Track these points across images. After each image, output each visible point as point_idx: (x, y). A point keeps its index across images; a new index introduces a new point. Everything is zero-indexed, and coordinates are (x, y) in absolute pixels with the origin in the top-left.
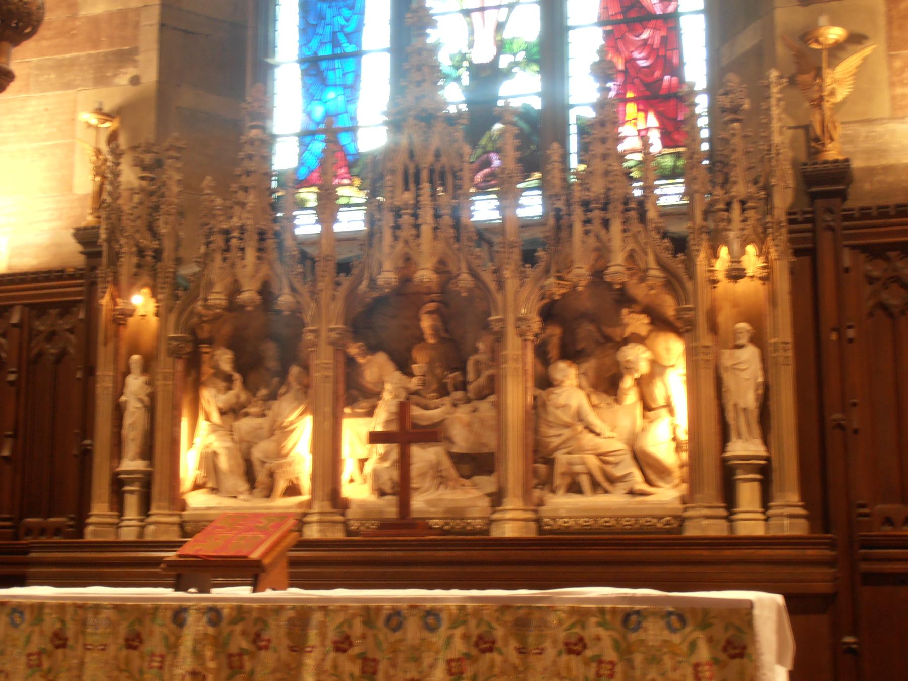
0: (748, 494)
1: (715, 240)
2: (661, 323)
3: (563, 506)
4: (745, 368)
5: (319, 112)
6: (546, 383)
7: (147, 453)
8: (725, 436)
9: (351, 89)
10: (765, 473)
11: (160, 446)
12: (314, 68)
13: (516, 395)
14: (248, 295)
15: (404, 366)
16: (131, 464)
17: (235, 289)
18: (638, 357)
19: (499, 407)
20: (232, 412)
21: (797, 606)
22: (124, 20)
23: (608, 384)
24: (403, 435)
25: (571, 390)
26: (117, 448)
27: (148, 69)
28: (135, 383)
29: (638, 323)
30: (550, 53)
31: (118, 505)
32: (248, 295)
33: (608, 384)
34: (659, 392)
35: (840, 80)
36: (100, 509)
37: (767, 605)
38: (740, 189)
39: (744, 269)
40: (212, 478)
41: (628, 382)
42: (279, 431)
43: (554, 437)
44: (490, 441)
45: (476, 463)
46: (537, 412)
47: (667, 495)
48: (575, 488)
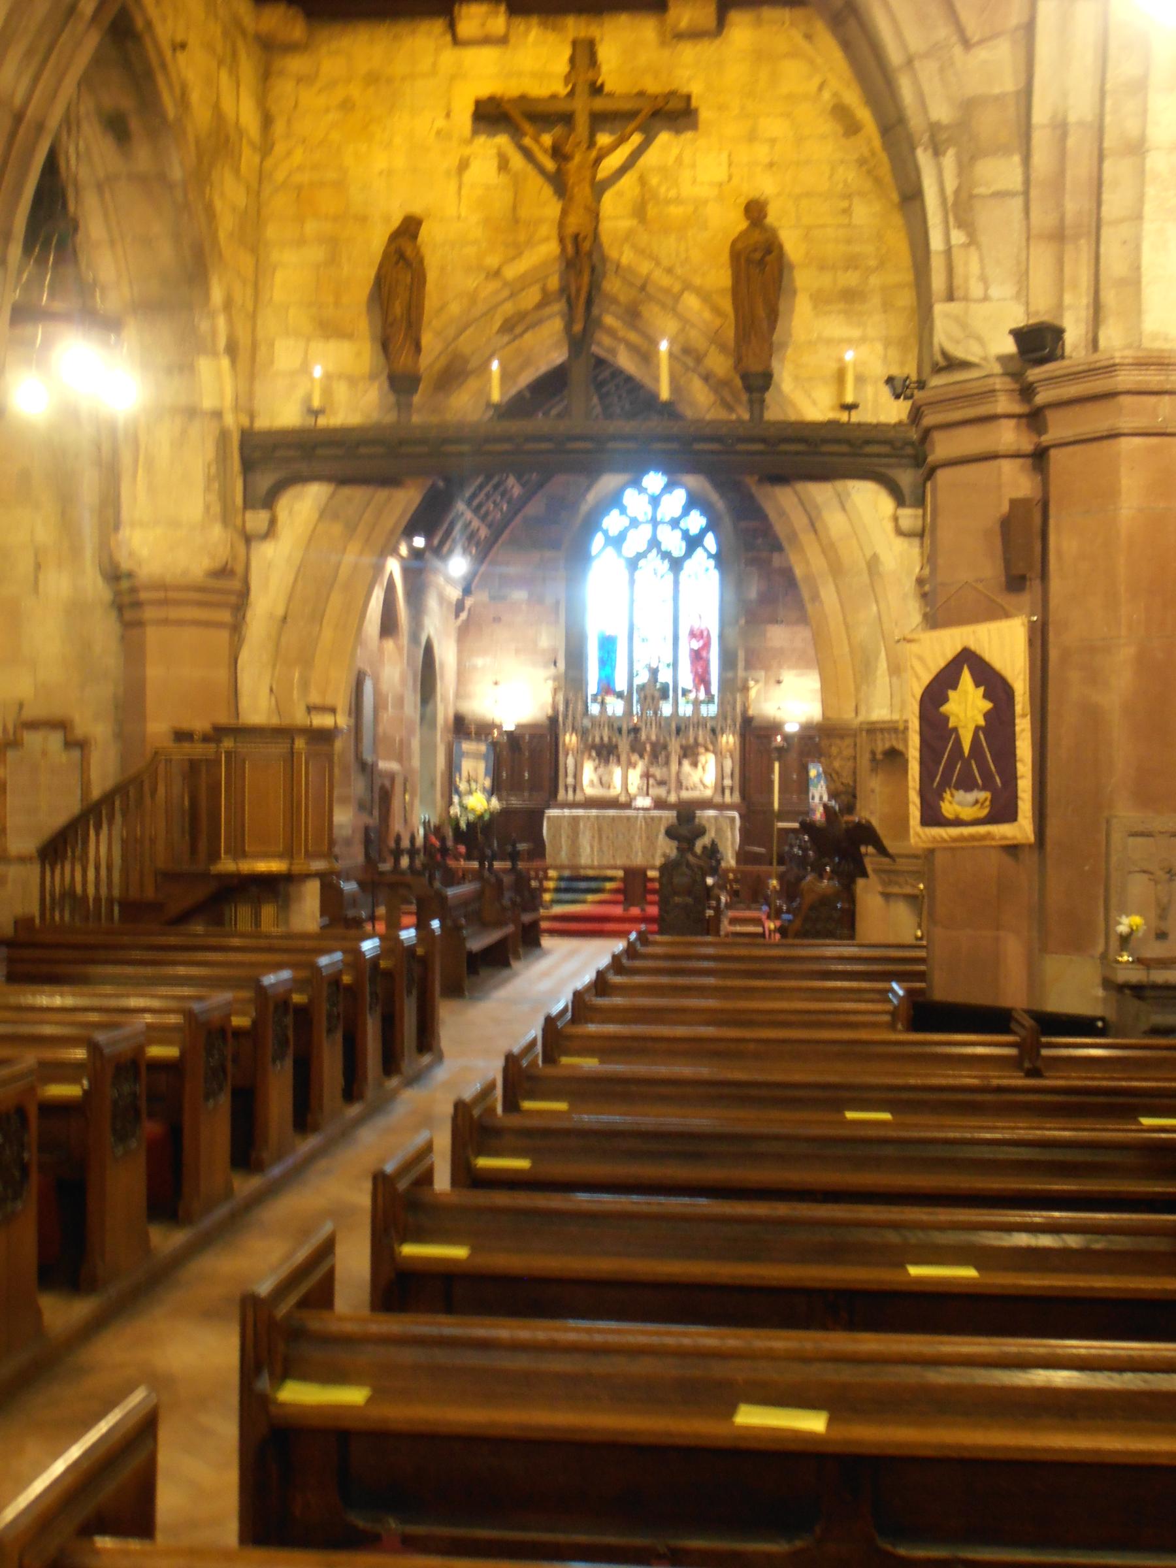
0: (727, 792)
1: (723, 732)
2: (707, 750)
3: (685, 795)
4: (728, 764)
5: (603, 675)
6: (680, 763)
7: (575, 776)
8: (723, 778)
9: (613, 668)
10: (732, 789)
11: (577, 775)
12: (603, 663)
13: (674, 767)
14: (606, 739)
15: (641, 756)
16: (570, 780)
17: (602, 738)
18: (702, 759)
19: (669, 771)
20: (596, 769)
21: (741, 817)
22: (554, 651)
23: (695, 764)
24: (647, 775)
25: (686, 764)
26: (566, 775)
27: (562, 665)
28: (570, 761)
29: (702, 750)
30: (675, 665)
31: (566, 791)
32: (606, 739)
33: (695, 764)
34: (707, 767)
35: (753, 693)
36: (561, 792)
37: (736, 814)
38: (729, 722)
39: (729, 740)
40: (592, 784)
41: (700, 766)
42: (611, 773)
43: (682, 777)
44: (666, 778)
45: (662, 783)
46: (678, 773)
47: (708, 793)
48: (687, 789)
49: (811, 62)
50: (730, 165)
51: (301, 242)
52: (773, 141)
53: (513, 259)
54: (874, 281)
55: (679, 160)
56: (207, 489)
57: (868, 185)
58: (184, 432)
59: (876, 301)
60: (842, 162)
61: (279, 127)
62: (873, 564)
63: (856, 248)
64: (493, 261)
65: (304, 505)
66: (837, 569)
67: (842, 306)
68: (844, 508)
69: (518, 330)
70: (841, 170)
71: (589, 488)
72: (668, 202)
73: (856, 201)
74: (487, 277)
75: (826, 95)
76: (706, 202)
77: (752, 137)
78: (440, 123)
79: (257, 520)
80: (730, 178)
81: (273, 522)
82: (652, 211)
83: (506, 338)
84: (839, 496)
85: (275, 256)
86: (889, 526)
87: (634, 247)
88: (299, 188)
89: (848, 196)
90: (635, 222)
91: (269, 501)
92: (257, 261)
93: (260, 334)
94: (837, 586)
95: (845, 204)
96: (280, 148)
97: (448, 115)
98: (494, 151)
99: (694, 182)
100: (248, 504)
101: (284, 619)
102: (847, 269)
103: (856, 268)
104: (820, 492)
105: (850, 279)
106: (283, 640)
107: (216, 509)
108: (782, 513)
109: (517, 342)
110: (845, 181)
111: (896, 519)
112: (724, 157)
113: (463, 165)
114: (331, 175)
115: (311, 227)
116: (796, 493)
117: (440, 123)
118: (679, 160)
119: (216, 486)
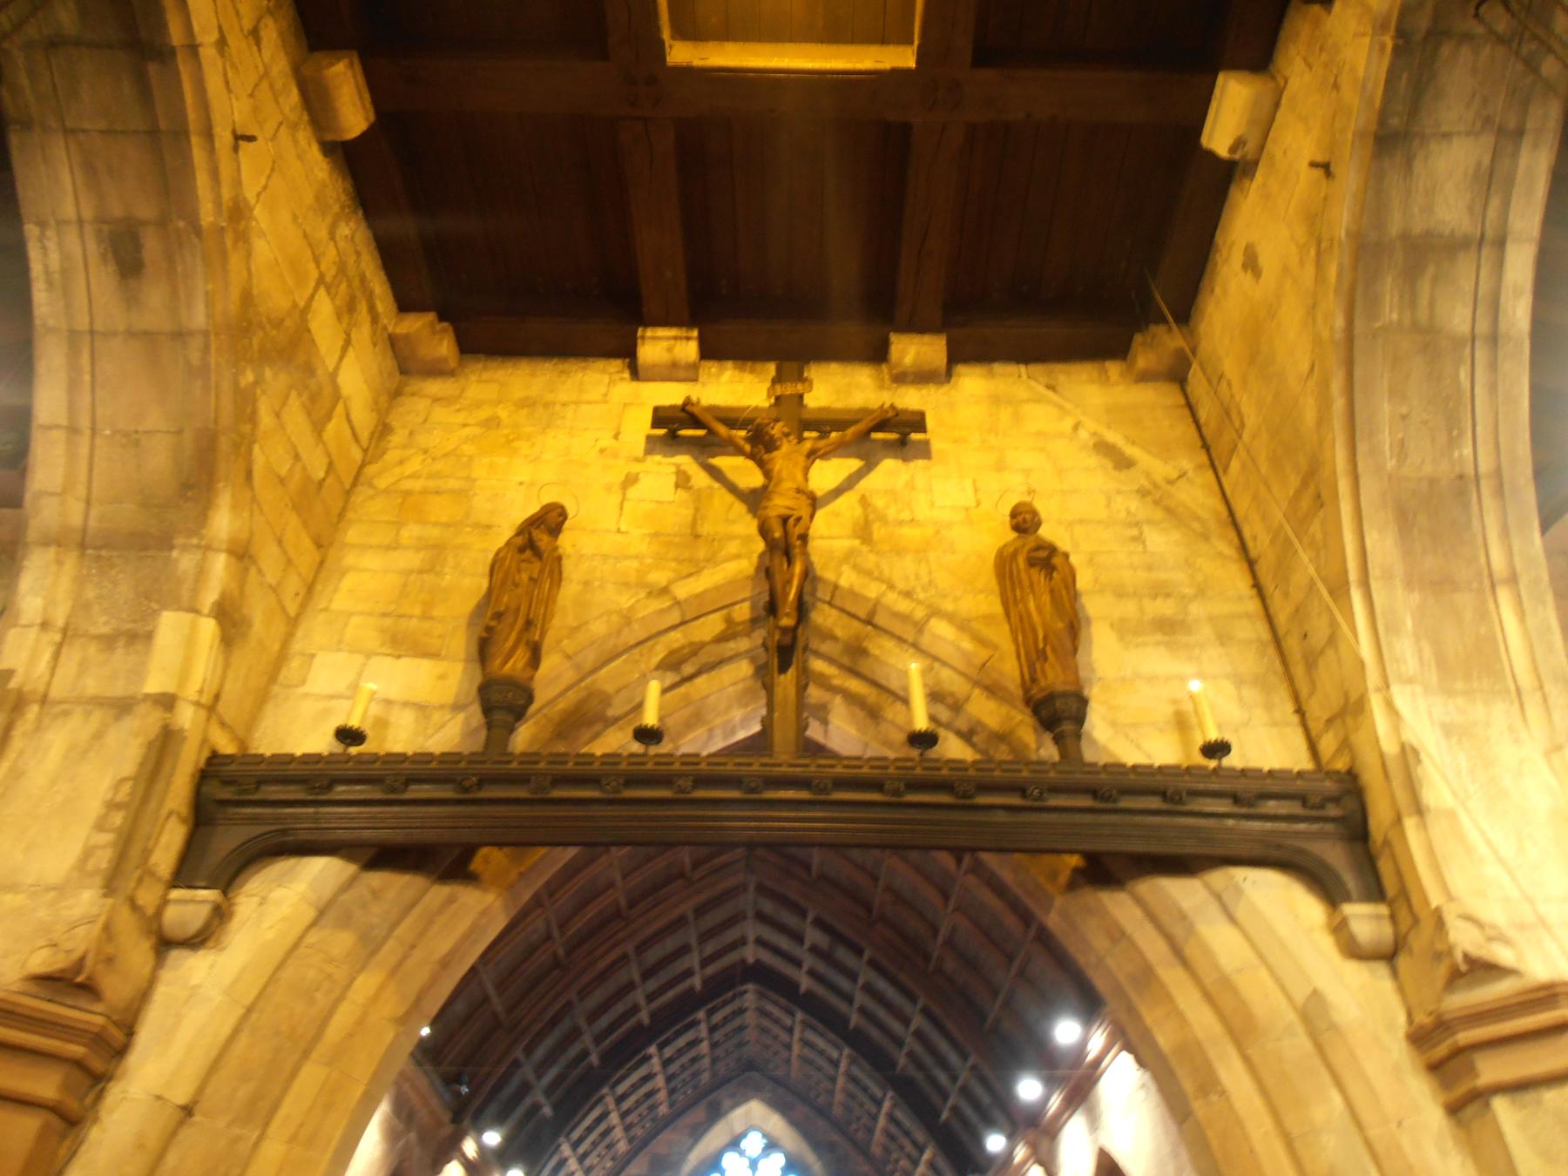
49: (1061, 407)
50: (976, 491)
51: (394, 546)
52: (1027, 472)
53: (690, 575)
54: (1196, 610)
55: (911, 485)
56: (100, 826)
57: (1158, 514)
58: (98, 736)
59: (1206, 632)
60: (1119, 492)
61: (396, 439)
62: (1313, 1014)
63: (1162, 576)
64: (659, 577)
65: (289, 895)
66: (1241, 1028)
67: (1159, 637)
68: (1232, 919)
69: (688, 669)
70: (1119, 499)
71: (691, 1148)
72: (901, 523)
73: (1146, 529)
74: (650, 593)
75: (1083, 434)
76: (950, 525)
77: (1000, 467)
78: (607, 441)
79: (189, 907)
80: (978, 504)
81: (221, 914)
82: (878, 532)
83: (671, 678)
84: (1218, 897)
85: (350, 559)
86: (1327, 943)
87: (855, 567)
88: (408, 493)
89: (1137, 524)
90: (857, 542)
91: (228, 877)
92: (322, 563)
93: (297, 646)
94: (1246, 1059)
95: (1135, 532)
96: (392, 456)
97: (616, 436)
98: (673, 469)
99: (932, 505)
100: (184, 875)
101: (188, 1111)
102: (1155, 597)
103: (1168, 596)
104: (1183, 892)
105: (1166, 608)
106: (171, 1159)
107: (103, 859)
108: (1118, 935)
109: (682, 690)
110: (1128, 512)
111: (1339, 929)
112: (968, 484)
113: (630, 481)
114: (453, 484)
115: (410, 532)
116: (1139, 901)
117: (607, 441)
118: (911, 485)
119: (118, 819)
